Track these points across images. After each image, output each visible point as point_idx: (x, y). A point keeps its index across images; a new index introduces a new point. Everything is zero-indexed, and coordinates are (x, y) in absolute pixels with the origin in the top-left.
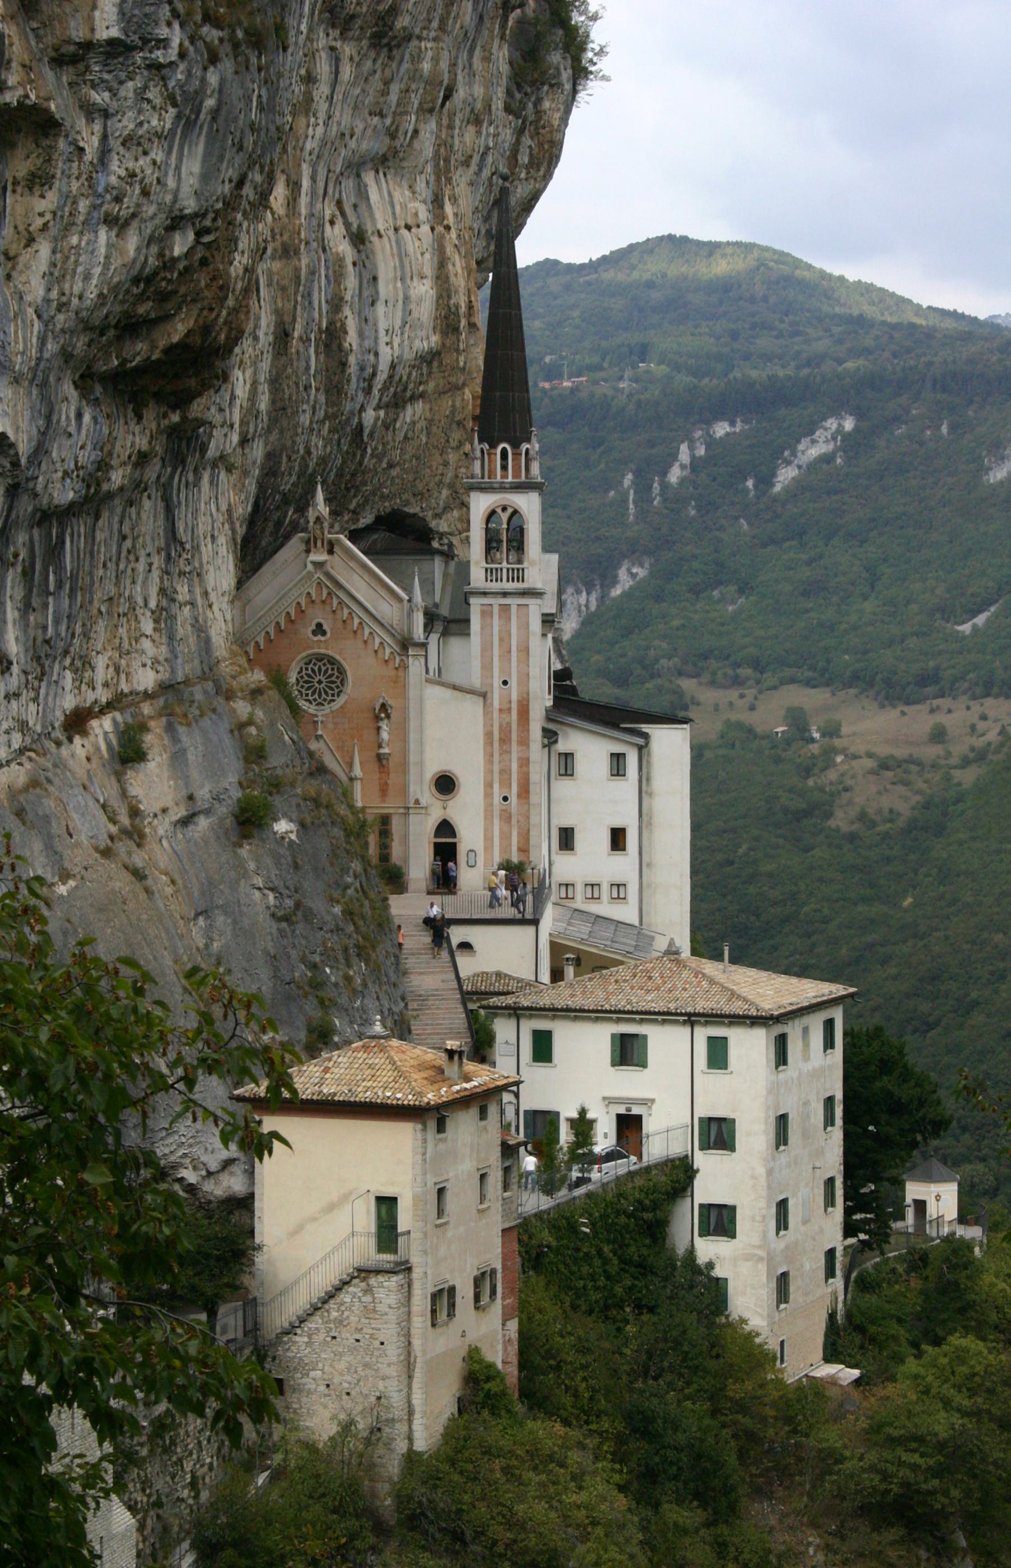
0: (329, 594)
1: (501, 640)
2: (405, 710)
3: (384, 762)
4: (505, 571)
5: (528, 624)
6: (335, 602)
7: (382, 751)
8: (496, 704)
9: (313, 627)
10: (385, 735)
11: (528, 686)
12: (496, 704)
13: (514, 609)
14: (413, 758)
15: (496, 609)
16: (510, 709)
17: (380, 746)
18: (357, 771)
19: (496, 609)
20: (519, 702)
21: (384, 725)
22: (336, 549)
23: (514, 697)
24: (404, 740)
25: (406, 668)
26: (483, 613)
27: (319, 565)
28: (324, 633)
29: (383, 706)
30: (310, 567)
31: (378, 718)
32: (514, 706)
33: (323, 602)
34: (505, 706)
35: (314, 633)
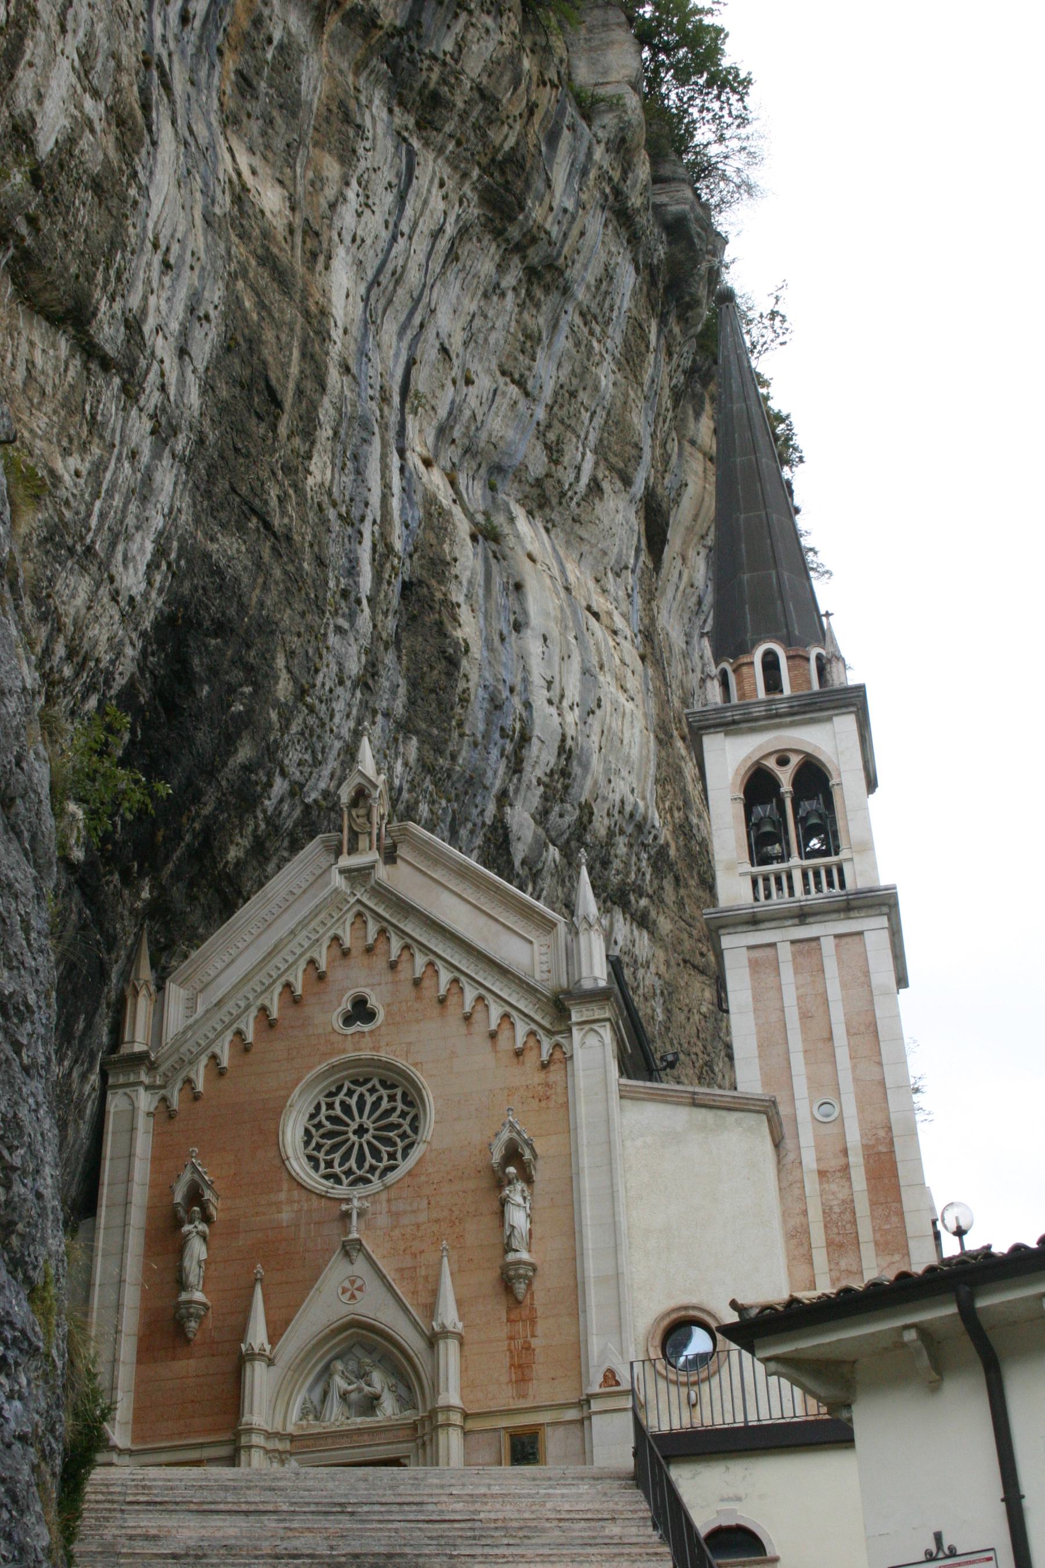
0: (382, 932)
1: (805, 1016)
2: (569, 1159)
3: (520, 1287)
4: (797, 876)
5: (867, 974)
6: (396, 944)
7: (511, 1257)
8: (809, 1159)
9: (347, 1005)
10: (518, 1217)
11: (886, 1109)
12: (809, 1159)
13: (828, 946)
14: (593, 1267)
15: (785, 952)
16: (846, 1168)
17: (508, 1248)
18: (449, 1315)
19: (785, 952)
20: (865, 1147)
21: (516, 1193)
22: (402, 851)
23: (854, 1137)
24: (572, 1231)
25: (563, 1058)
26: (755, 966)
27: (358, 875)
28: (369, 1016)
29: (513, 1154)
30: (338, 881)
31: (500, 1182)
32: (856, 1160)
33: (369, 950)
34: (834, 1163)
35: (348, 1020)
